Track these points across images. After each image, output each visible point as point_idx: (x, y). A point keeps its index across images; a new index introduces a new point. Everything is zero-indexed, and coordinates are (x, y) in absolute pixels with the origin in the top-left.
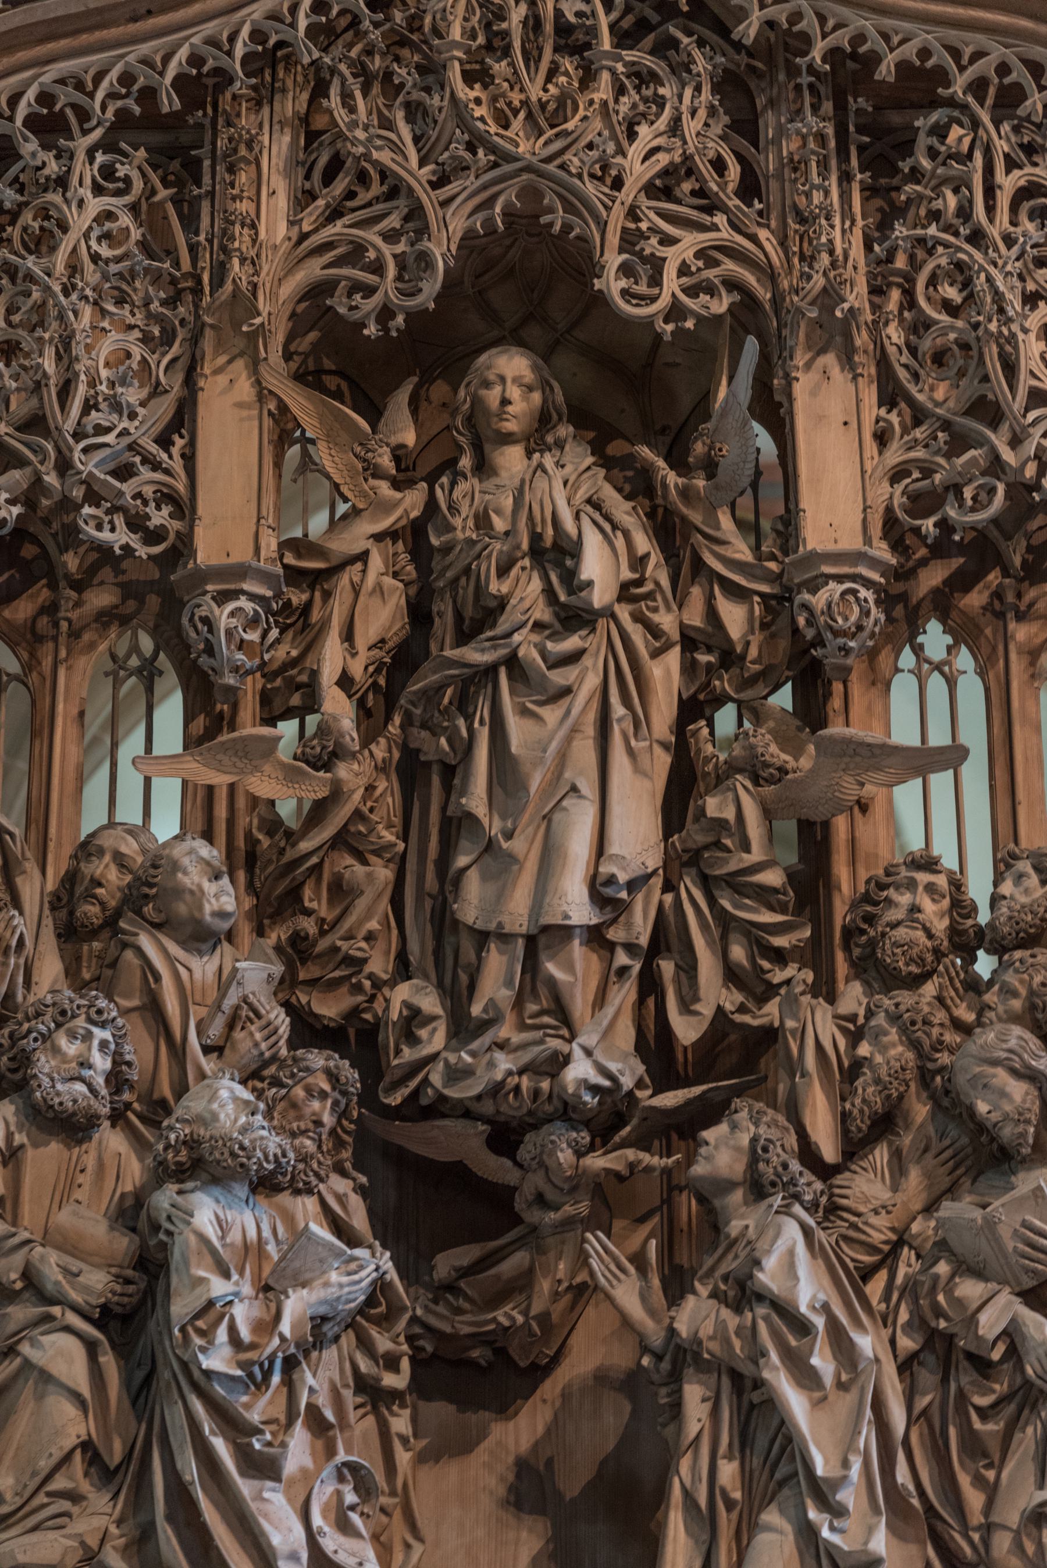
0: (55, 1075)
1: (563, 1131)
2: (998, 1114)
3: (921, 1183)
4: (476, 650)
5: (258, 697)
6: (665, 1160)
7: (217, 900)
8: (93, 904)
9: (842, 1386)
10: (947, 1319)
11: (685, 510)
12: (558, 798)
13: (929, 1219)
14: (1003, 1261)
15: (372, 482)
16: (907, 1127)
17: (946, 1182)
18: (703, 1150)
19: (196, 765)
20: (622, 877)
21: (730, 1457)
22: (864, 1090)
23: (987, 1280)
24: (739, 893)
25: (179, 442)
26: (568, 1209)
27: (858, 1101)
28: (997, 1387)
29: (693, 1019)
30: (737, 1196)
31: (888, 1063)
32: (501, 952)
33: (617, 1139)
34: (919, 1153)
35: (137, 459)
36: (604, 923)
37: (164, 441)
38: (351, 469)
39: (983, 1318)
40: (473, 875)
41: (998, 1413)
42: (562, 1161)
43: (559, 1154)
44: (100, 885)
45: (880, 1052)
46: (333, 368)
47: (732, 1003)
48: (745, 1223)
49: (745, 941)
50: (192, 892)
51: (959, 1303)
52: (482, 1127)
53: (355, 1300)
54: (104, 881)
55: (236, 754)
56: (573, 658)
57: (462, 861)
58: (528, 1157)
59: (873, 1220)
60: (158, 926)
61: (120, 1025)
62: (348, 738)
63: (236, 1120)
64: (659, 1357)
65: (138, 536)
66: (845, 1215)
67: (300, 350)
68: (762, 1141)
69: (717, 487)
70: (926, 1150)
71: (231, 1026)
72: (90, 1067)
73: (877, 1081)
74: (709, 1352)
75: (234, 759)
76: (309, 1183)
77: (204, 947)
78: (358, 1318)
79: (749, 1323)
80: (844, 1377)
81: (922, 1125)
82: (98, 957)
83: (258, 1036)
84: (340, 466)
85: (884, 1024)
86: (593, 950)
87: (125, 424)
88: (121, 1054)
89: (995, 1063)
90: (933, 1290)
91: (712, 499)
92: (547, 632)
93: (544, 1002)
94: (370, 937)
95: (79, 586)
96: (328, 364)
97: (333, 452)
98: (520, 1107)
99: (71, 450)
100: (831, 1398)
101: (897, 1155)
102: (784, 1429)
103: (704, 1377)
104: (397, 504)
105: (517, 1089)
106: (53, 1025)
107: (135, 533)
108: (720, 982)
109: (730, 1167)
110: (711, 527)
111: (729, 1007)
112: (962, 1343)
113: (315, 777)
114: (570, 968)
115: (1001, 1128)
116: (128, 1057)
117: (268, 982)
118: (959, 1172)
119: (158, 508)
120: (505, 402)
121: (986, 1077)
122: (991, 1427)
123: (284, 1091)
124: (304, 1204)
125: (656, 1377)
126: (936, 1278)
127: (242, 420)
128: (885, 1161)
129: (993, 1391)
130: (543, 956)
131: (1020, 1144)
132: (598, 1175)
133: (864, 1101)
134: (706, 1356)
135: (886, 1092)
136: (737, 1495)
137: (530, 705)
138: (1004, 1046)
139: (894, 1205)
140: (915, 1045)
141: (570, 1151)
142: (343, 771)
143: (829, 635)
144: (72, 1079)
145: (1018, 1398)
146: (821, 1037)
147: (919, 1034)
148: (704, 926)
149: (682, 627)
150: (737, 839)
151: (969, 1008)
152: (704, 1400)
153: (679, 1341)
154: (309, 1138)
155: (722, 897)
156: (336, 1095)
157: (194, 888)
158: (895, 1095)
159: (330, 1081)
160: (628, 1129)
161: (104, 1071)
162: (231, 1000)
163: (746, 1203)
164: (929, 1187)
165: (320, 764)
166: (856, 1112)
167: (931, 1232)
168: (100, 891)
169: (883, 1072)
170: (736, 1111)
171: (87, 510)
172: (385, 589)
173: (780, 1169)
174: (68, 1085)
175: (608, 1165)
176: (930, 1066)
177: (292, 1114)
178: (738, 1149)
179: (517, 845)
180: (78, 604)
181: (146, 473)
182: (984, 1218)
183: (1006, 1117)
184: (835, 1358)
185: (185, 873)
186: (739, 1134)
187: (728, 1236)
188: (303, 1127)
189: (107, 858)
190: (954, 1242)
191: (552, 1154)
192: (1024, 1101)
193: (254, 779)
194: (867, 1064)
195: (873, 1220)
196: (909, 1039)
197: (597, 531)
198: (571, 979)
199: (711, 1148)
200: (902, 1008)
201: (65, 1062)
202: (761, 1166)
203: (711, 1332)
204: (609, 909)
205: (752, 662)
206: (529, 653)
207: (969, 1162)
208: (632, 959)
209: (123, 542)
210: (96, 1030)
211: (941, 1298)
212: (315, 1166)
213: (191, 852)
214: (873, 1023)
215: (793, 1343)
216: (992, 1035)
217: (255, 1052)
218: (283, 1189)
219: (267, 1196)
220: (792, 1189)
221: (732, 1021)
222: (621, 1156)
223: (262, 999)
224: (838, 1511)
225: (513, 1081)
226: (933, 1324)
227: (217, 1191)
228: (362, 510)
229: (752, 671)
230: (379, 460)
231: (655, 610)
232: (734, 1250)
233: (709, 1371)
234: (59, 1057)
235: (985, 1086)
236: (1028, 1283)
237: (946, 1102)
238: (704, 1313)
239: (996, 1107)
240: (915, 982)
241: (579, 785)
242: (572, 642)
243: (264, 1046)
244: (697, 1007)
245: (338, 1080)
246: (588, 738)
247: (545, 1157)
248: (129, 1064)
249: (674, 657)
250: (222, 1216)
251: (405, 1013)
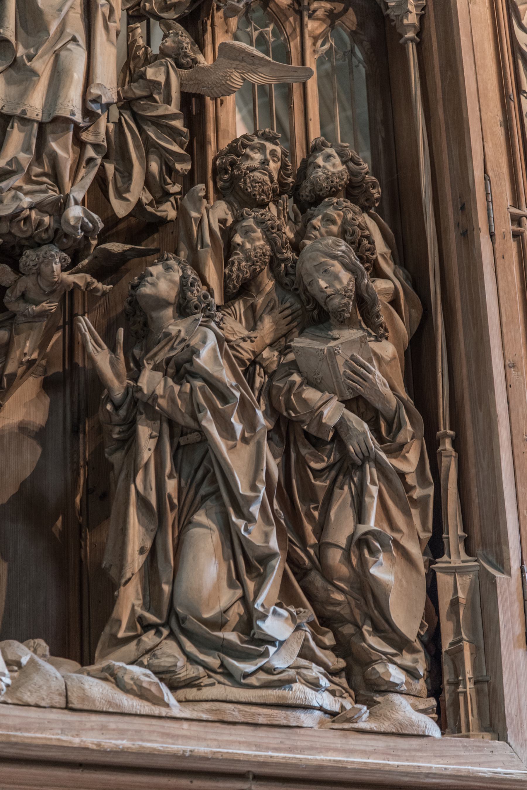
2: (332, 290)
3: (272, 326)
6: (105, 286)
9: (245, 440)
10: (295, 411)
13: (273, 351)
14: (334, 380)
16: (259, 292)
17: (284, 330)
18: (149, 279)
21: (171, 476)
22: (239, 264)
23: (322, 391)
26: (45, 305)
27: (235, 269)
28: (326, 459)
30: (170, 312)
31: (255, 249)
34: (268, 309)
39: (327, 411)
41: (322, 476)
42: (55, 270)
43: (54, 265)
45: (249, 242)
48: (179, 328)
51: (305, 402)
58: (32, 263)
64: (117, 408)
68: (191, 279)
70: (272, 308)
73: (248, 259)
74: (159, 406)
79: (188, 390)
80: (247, 435)
81: (269, 293)
89: (334, 257)
90: (289, 391)
100: (238, 446)
101: (252, 309)
102: (205, 463)
103: (151, 423)
112: (305, 427)
115: (331, 299)
118: (295, 324)
121: (328, 265)
122: (318, 483)
125: (116, 419)
126: (293, 383)
128: (242, 311)
129: (323, 461)
131: (343, 311)
132: (69, 286)
133: (239, 269)
134: (157, 408)
135: (254, 267)
136: (176, 501)
138: (340, 249)
140: (270, 241)
141: (59, 265)
145: (336, 467)
147: (275, 235)
151: (291, 230)
152: (151, 437)
153: (138, 395)
158: (258, 270)
163: (174, 317)
164: (276, 330)
166: (234, 276)
167: (275, 359)
169: (252, 253)
170: (167, 260)
173: (202, 298)
176: (279, 256)
178: (172, 281)
182: (329, 350)
183: (337, 292)
184: (241, 422)
187: (167, 335)
190: (302, 364)
191: (50, 263)
192: (348, 284)
194: (239, 248)
196: (267, 237)
199: (154, 278)
202: (189, 294)
203: (162, 393)
207: (299, 320)
211: (292, 397)
214: (244, 224)
215: (220, 407)
216: (330, 241)
220: (208, 313)
224: (250, 519)
226: (285, 414)
232: (170, 344)
233: (154, 419)
235: (326, 271)
236: (348, 396)
237: (287, 280)
238: (158, 380)
239: (331, 285)
240: (264, 205)
247: (42, 266)
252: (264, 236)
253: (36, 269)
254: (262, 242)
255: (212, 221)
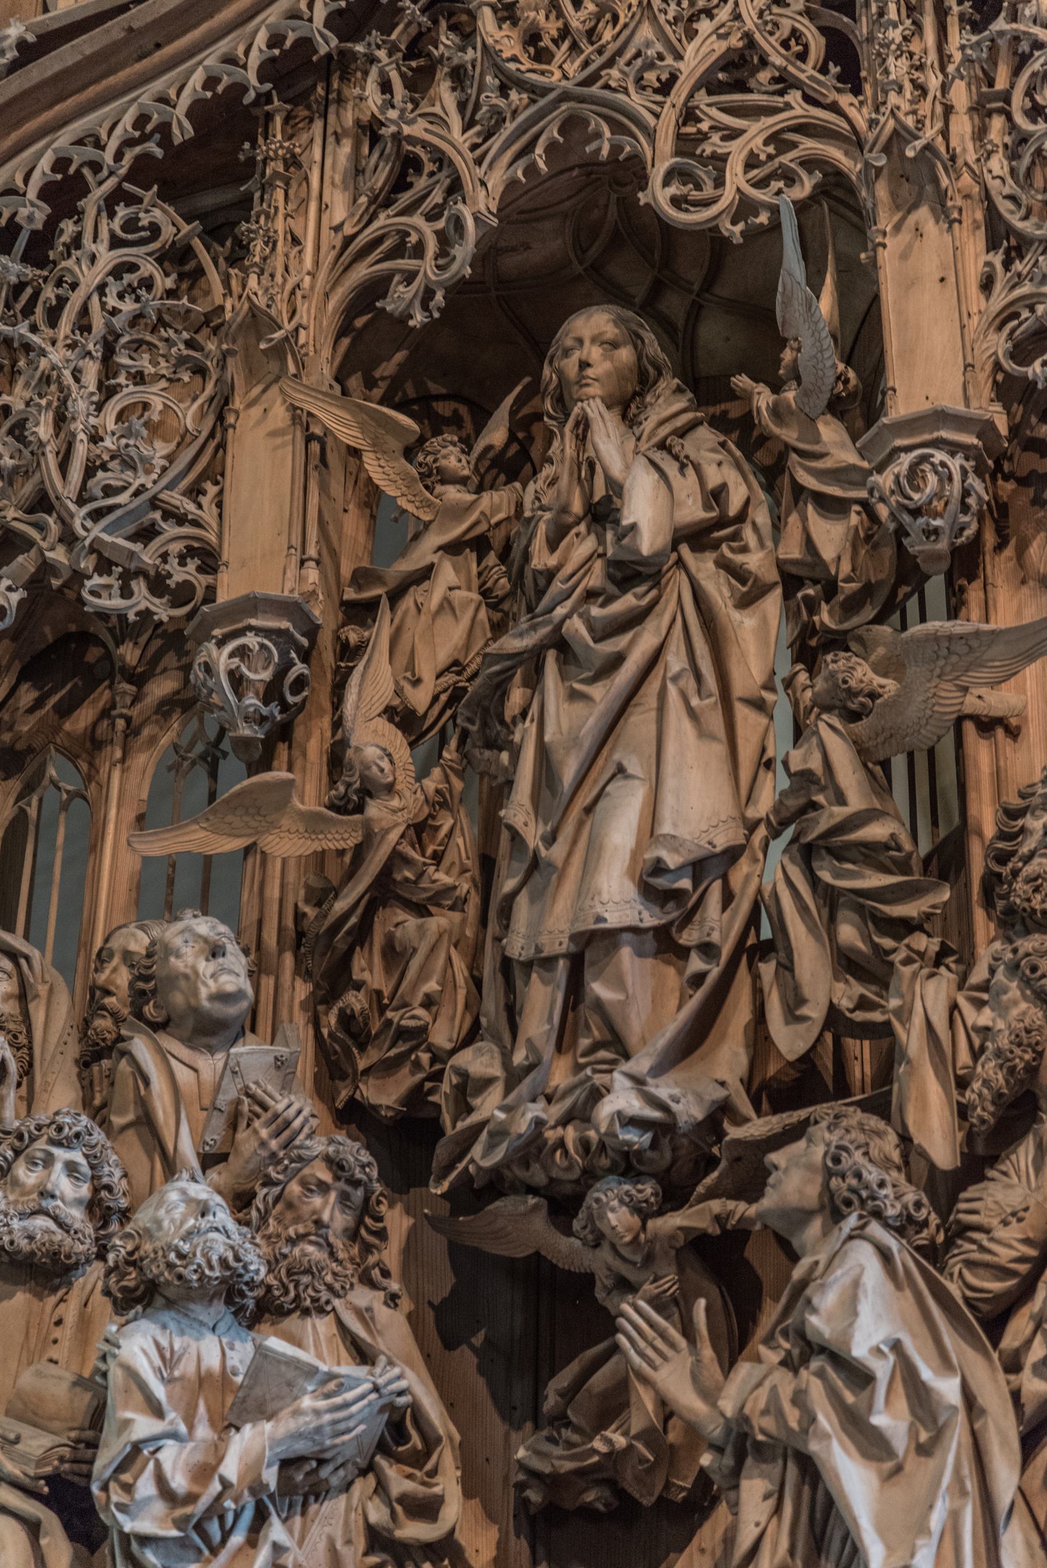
0: (12, 1211)
1: (613, 1185)
4: (515, 636)
5: (325, 759)
7: (216, 981)
8: (104, 1017)
11: (776, 430)
12: (601, 783)
15: (439, 488)
19: (202, 834)
20: (672, 860)
24: (841, 859)
25: (212, 490)
29: (801, 1027)
32: (545, 982)
33: (700, 1189)
35: (157, 515)
36: (671, 924)
37: (195, 492)
38: (405, 476)
40: (522, 901)
42: (614, 1223)
43: (610, 1215)
44: (108, 993)
46: (444, 391)
47: (850, 998)
49: (855, 917)
50: (186, 977)
52: (532, 1201)
53: (349, 1431)
54: (112, 988)
55: (247, 813)
56: (635, 620)
57: (509, 885)
59: (1001, 1233)
60: (157, 1027)
61: (94, 1142)
62: (375, 769)
63: (182, 1223)
65: (164, 600)
66: (976, 1235)
67: (386, 374)
69: (806, 394)
71: (233, 1126)
72: (53, 1197)
75: (246, 819)
76: (318, 1300)
77: (213, 1041)
78: (378, 1458)
82: (107, 1077)
83: (264, 1133)
84: (393, 476)
85: (1005, 980)
86: (668, 963)
87: (142, 479)
88: (100, 1177)
91: (807, 410)
92: (601, 599)
93: (596, 1033)
94: (429, 1002)
95: (139, 679)
96: (434, 388)
97: (382, 463)
98: (570, 1168)
99: (72, 516)
104: (471, 506)
105: (561, 1143)
106: (9, 1154)
107: (160, 596)
108: (830, 973)
109: (800, 1192)
110: (808, 442)
111: (845, 1004)
113: (341, 822)
114: (619, 983)
116: (105, 1180)
117: (278, 1068)
119: (182, 563)
120: (584, 365)
123: (276, 1190)
124: (314, 1327)
127: (275, 449)
130: (588, 975)
137: (577, 686)
139: (1026, 1209)
141: (624, 1209)
142: (374, 809)
143: (906, 518)
144: (34, 1213)
146: (929, 1012)
148: (803, 909)
149: (780, 565)
150: (831, 792)
154: (311, 1243)
155: (821, 868)
156: (341, 1185)
157: (188, 971)
159: (330, 1169)
160: (715, 1174)
161: (78, 1202)
162: (230, 1092)
165: (350, 807)
168: (110, 1001)
171: (97, 580)
172: (456, 604)
174: (26, 1223)
175: (686, 1223)
177: (289, 1216)
179: (557, 852)
180: (136, 699)
181: (171, 530)
185: (178, 956)
186: (813, 1148)
188: (301, 1230)
189: (116, 961)
191: (603, 1217)
193: (271, 838)
195: (1001, 1233)
197: (652, 470)
198: (621, 997)
200: (1021, 952)
201: (23, 1194)
204: (671, 905)
205: (846, 581)
206: (577, 626)
208: (708, 963)
209: (142, 606)
210: (57, 1152)
212: (329, 1278)
213: (188, 929)
217: (264, 1153)
218: (290, 1312)
219: (273, 1324)
221: (851, 1020)
222: (703, 1210)
223: (270, 1088)
225: (551, 1135)
227: (173, 1314)
228: (431, 522)
229: (847, 592)
230: (443, 462)
231: (745, 550)
234: (18, 1190)
241: (625, 763)
242: (628, 601)
243: (274, 1144)
244: (804, 1011)
245: (342, 1168)
246: (650, 710)
248: (109, 1188)
249: (772, 604)
250: (164, 1343)
251: (455, 1081)
252: (1028, 992)
253: (592, 1232)
254: (1024, 1006)
255: (929, 1004)
